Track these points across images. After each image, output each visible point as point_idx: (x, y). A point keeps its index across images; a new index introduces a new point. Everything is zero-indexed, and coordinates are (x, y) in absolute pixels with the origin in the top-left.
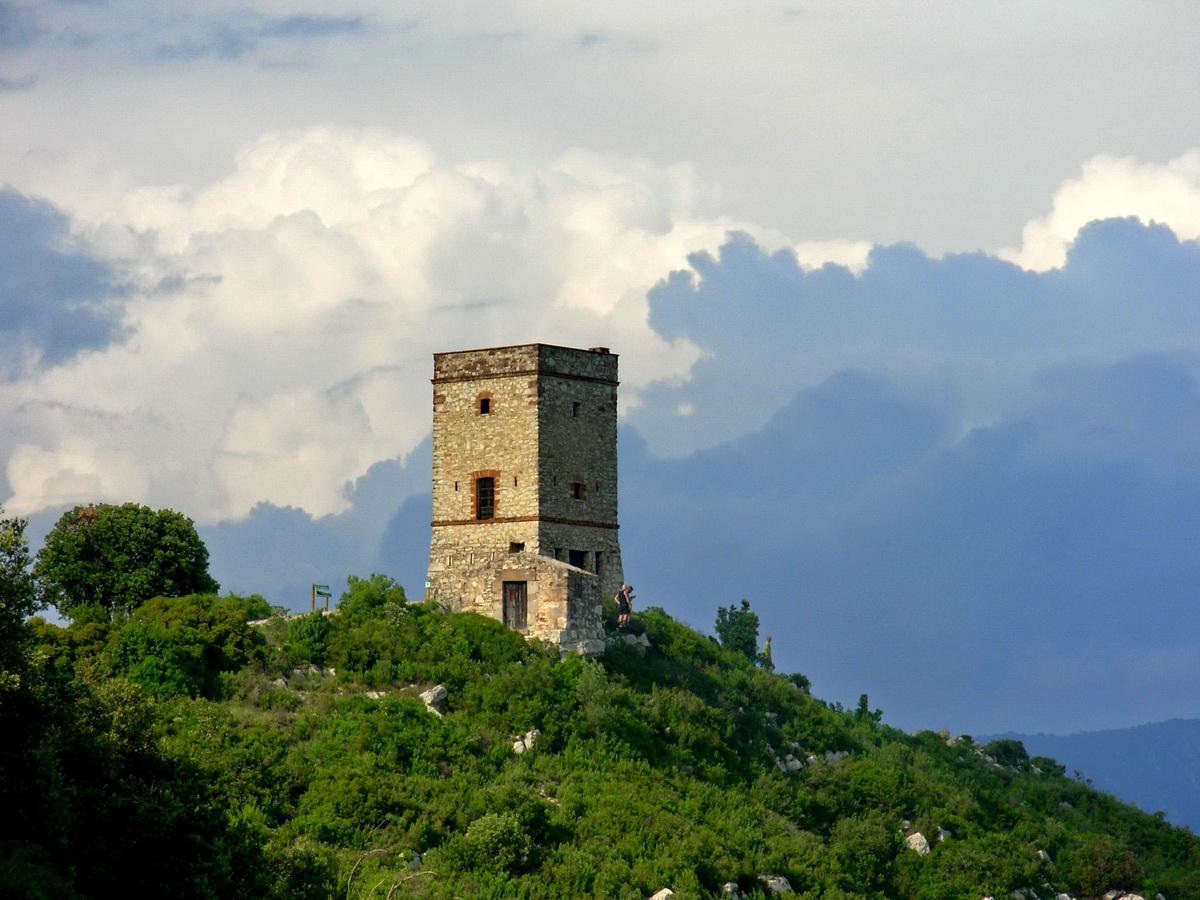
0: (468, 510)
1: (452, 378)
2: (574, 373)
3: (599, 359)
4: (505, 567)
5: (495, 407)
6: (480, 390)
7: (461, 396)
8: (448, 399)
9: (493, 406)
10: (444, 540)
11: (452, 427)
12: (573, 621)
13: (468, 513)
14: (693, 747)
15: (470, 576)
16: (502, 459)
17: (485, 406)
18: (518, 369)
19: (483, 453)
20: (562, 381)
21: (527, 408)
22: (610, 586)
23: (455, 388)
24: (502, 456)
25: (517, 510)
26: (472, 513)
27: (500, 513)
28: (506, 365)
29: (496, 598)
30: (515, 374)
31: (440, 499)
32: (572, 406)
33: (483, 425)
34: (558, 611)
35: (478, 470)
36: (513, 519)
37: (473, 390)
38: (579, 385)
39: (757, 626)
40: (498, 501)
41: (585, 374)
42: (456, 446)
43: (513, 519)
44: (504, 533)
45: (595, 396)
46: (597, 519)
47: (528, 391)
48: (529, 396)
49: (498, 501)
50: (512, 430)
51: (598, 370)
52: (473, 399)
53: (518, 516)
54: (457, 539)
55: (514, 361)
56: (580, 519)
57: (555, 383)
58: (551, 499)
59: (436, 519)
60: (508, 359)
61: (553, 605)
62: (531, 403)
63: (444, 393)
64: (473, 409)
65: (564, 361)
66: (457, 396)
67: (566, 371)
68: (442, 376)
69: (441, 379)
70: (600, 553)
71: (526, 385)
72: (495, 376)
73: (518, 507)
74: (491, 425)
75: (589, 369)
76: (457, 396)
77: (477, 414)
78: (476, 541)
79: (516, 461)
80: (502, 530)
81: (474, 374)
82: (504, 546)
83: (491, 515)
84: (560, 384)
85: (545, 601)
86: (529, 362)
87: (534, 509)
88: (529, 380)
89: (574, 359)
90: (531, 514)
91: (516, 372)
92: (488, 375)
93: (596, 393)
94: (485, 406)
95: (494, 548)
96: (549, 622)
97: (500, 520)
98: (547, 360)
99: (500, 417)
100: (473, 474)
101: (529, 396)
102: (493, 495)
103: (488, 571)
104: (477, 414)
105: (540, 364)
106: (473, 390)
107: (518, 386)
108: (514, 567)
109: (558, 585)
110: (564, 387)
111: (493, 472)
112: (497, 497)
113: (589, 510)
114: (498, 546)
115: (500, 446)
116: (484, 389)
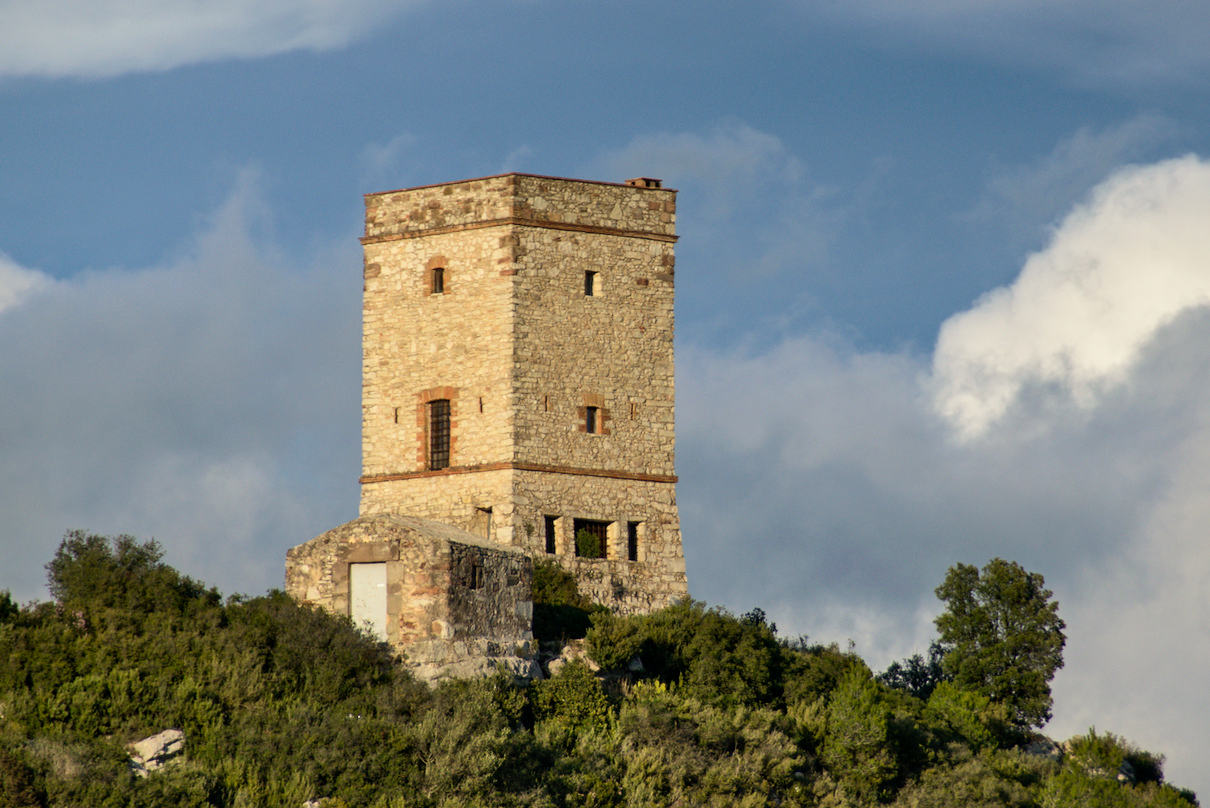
0: (413, 455)
1: (390, 234)
2: (588, 222)
3: (636, 197)
4: (352, 540)
5: (451, 280)
6: (432, 252)
7: (404, 265)
8: (385, 271)
9: (449, 280)
10: (378, 507)
11: (390, 317)
12: (458, 627)
13: (413, 460)
14: (502, 791)
15: (298, 556)
16: (460, 367)
17: (438, 279)
18: (484, 217)
19: (435, 360)
20: (561, 234)
21: (495, 281)
22: (656, 579)
23: (394, 250)
24: (461, 363)
25: (482, 453)
26: (419, 459)
27: (457, 459)
28: (467, 211)
29: (339, 591)
30: (480, 224)
31: (374, 439)
32: (582, 277)
33: (435, 311)
34: (433, 611)
35: (428, 387)
36: (477, 468)
37: (421, 254)
38: (597, 241)
39: (54, 563)
40: (456, 439)
41: (609, 224)
42: (395, 349)
43: (477, 468)
44: (463, 492)
45: (630, 260)
46: (631, 468)
47: (500, 254)
48: (501, 261)
49: (456, 439)
50: (475, 318)
51: (638, 216)
52: (421, 268)
53: (484, 462)
54: (396, 504)
55: (480, 204)
56: (597, 466)
57: (547, 239)
58: (538, 433)
59: (367, 471)
60: (470, 200)
61: (426, 601)
62: (503, 273)
63: (378, 259)
64: (421, 286)
65: (566, 203)
66: (397, 263)
67: (570, 218)
68: (376, 232)
69: (374, 237)
70: (637, 523)
71: (496, 243)
72: (453, 228)
73: (485, 448)
74: (447, 312)
75: (616, 213)
76: (397, 263)
77: (426, 295)
78: (424, 508)
79: (482, 371)
80: (461, 486)
81: (422, 227)
82: (463, 513)
83: (446, 462)
84: (558, 239)
85: (414, 594)
86: (500, 204)
87: (505, 451)
88: (502, 235)
89: (584, 199)
90: (502, 458)
91: (481, 222)
92: (441, 228)
93: (630, 255)
94: (438, 279)
95: (450, 517)
96: (419, 628)
97: (457, 471)
98: (530, 201)
99: (458, 298)
100: (419, 395)
101: (501, 261)
102: (448, 429)
103: (325, 547)
104: (426, 295)
105: (518, 207)
106: (421, 254)
107: (485, 246)
108: (367, 539)
109: (435, 568)
110: (566, 246)
111: (448, 389)
112: (454, 432)
113: (616, 452)
114: (455, 513)
115: (461, 348)
116: (436, 251)
